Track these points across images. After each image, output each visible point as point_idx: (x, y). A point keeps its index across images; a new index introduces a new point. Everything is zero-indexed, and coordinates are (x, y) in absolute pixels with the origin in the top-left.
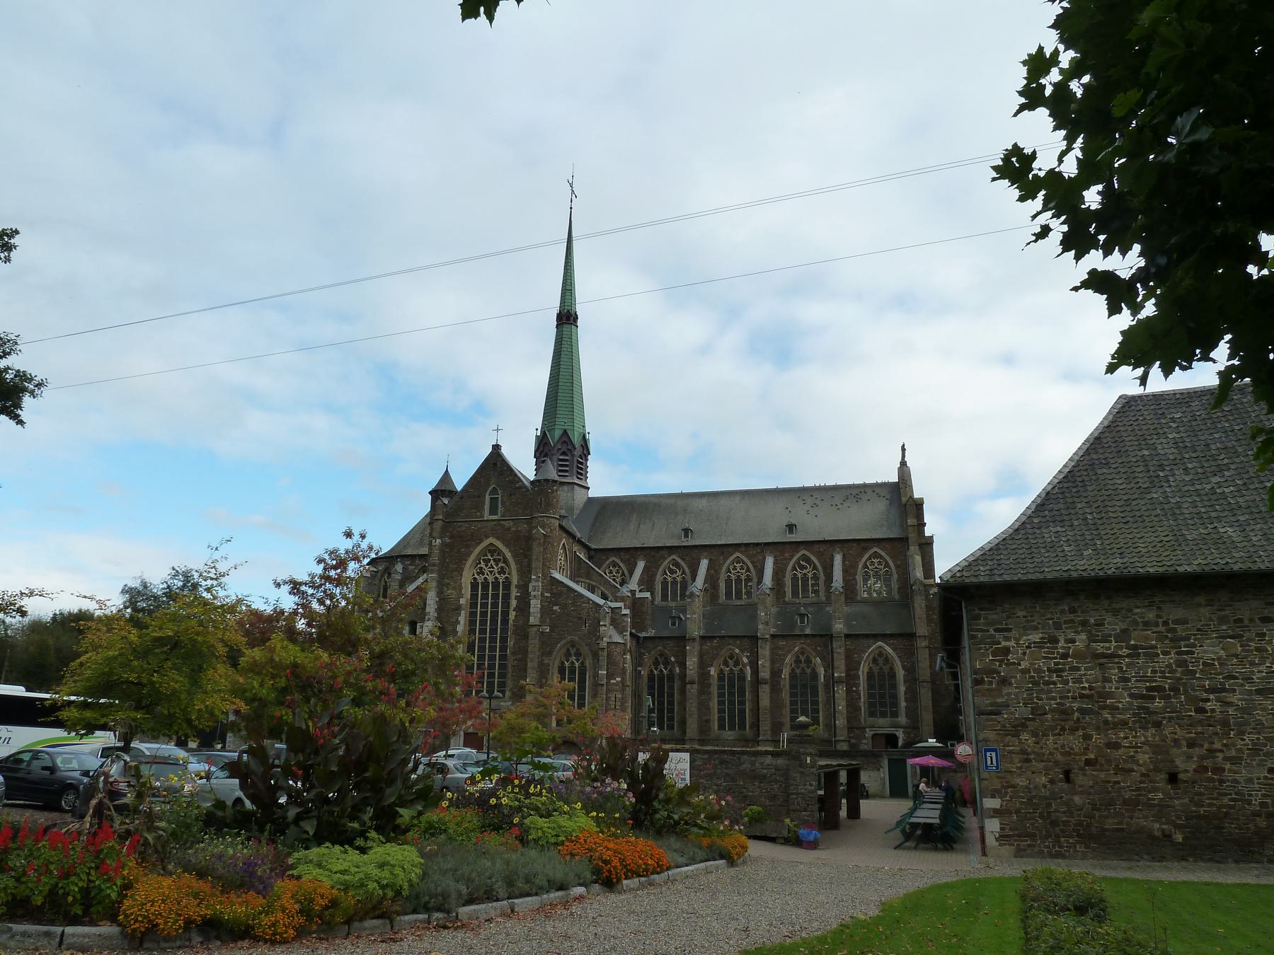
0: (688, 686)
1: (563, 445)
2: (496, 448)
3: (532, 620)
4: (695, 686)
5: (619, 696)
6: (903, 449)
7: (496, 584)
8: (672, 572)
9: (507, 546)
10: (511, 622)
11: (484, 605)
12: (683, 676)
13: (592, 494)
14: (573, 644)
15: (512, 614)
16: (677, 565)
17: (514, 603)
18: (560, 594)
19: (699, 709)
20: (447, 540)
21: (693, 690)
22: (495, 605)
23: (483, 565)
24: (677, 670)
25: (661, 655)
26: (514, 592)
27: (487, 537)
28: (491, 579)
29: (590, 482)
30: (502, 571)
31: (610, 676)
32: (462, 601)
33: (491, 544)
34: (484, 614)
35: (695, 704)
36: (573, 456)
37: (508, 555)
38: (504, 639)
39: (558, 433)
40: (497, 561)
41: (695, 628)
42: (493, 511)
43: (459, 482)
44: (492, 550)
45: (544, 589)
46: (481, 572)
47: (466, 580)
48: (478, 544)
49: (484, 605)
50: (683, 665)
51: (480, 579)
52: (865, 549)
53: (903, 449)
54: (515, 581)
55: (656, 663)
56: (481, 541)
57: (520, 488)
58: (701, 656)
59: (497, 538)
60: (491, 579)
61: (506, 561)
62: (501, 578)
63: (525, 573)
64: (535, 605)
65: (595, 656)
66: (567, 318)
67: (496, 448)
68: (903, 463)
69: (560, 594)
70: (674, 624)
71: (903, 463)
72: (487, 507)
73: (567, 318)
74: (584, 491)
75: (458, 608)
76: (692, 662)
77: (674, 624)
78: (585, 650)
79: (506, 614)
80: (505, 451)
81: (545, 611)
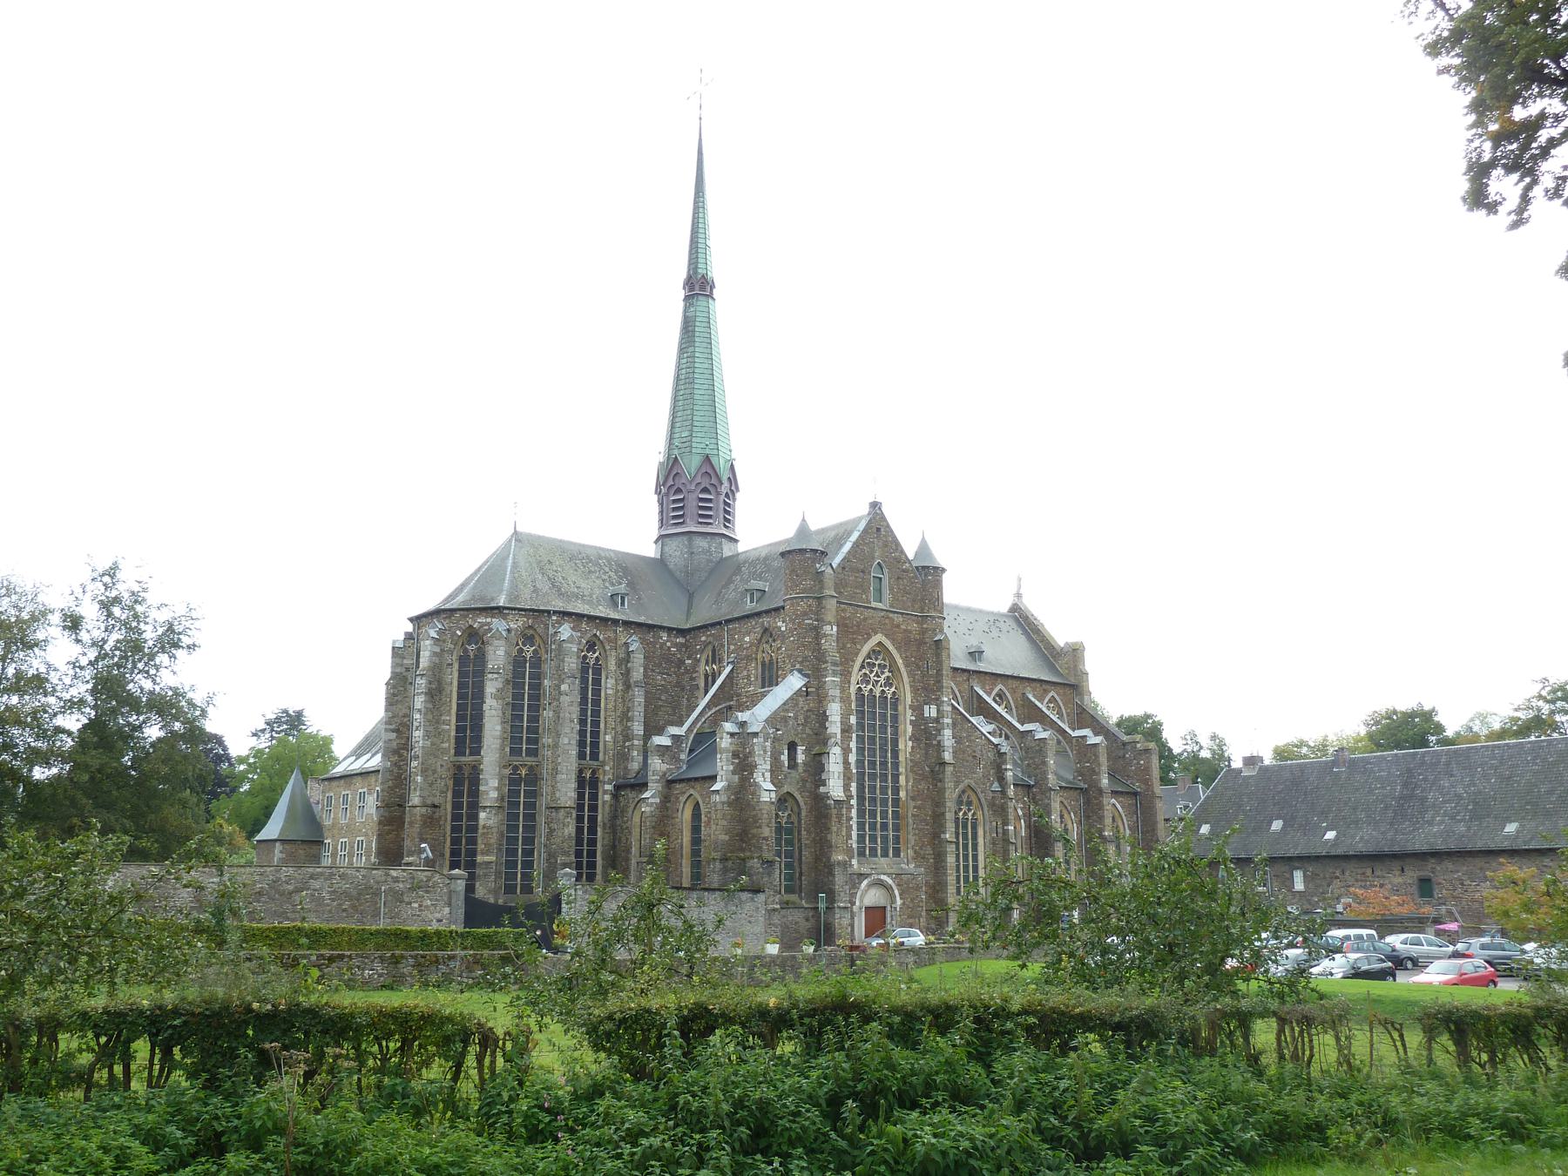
2: (875, 505)
30: (888, 683)
36: (718, 494)
37: (900, 662)
38: (896, 777)
39: (695, 462)
40: (882, 667)
51: (866, 689)
52: (1046, 692)
61: (893, 668)
62: (889, 692)
66: (698, 286)
67: (875, 505)
71: (1019, 595)
73: (698, 286)
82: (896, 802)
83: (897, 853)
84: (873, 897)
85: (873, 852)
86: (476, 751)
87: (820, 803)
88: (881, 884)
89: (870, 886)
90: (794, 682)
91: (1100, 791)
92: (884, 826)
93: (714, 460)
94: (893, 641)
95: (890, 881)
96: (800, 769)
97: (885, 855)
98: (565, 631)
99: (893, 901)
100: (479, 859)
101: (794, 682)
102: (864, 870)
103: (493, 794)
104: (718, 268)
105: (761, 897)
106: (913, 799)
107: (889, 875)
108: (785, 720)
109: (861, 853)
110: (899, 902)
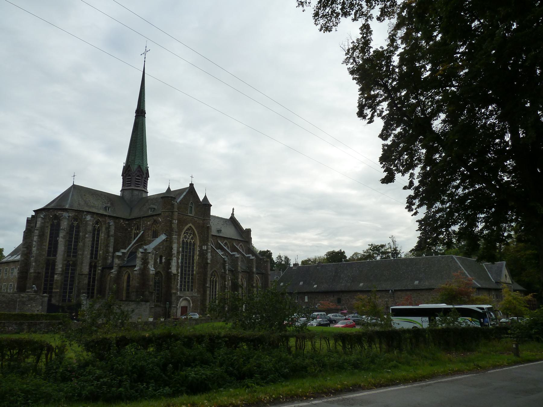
1: (135, 170)
2: (192, 185)
6: (233, 209)
7: (190, 243)
28: (189, 241)
30: (192, 239)
36: (142, 177)
37: (196, 232)
51: (185, 240)
52: (239, 243)
53: (233, 209)
60: (189, 241)
61: (194, 234)
66: (140, 113)
67: (192, 185)
68: (233, 214)
71: (233, 214)
73: (140, 113)
82: (193, 275)
83: (192, 290)
86: (55, 255)
87: (169, 276)
88: (186, 299)
89: (183, 300)
90: (163, 237)
91: (253, 273)
92: (188, 282)
93: (142, 167)
95: (189, 299)
96: (163, 264)
97: (188, 290)
98: (89, 218)
100: (54, 290)
101: (163, 237)
102: (181, 295)
103: (60, 270)
104: (147, 109)
105: (148, 304)
106: (198, 274)
108: (159, 248)
109: (181, 290)
110: (192, 305)
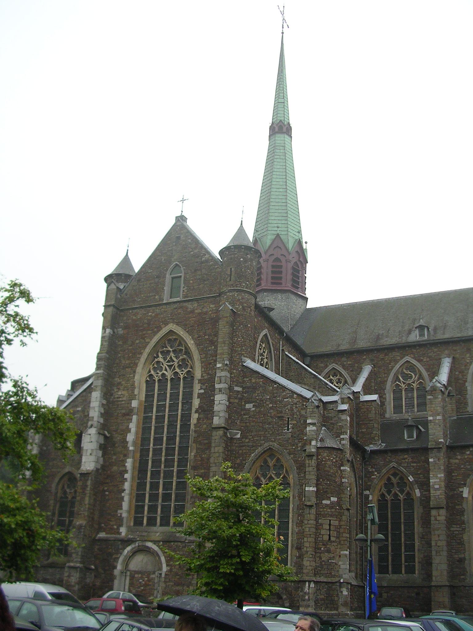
0: (434, 512)
2: (181, 220)
3: (216, 421)
4: (443, 512)
5: (335, 523)
7: (175, 380)
8: (407, 377)
9: (190, 332)
10: (192, 427)
11: (161, 408)
12: (426, 500)
13: (310, 305)
14: (270, 452)
15: (195, 417)
16: (412, 368)
17: (196, 402)
18: (254, 388)
19: (449, 544)
20: (120, 331)
21: (440, 517)
22: (173, 407)
23: (160, 359)
24: (417, 492)
25: (395, 475)
26: (197, 389)
27: (166, 324)
28: (169, 374)
29: (308, 294)
31: (320, 495)
32: (135, 404)
33: (171, 332)
34: (160, 419)
35: (443, 537)
37: (191, 343)
38: (184, 450)
41: (437, 434)
42: (173, 292)
43: (137, 265)
44: (171, 338)
45: (233, 381)
46: (158, 367)
47: (140, 377)
48: (155, 333)
49: (161, 408)
50: (425, 485)
54: (198, 374)
55: (389, 485)
56: (159, 329)
57: (207, 261)
58: (449, 473)
59: (177, 324)
60: (169, 374)
61: (188, 352)
63: (209, 366)
64: (220, 401)
65: (301, 467)
67: (181, 220)
69: (254, 388)
70: (411, 436)
72: (167, 289)
74: (301, 301)
75: (129, 413)
76: (437, 480)
77: (411, 436)
78: (288, 461)
79: (186, 417)
80: (193, 225)
81: (232, 409)
84: (139, 562)
85: (152, 522)
89: (134, 553)
94: (185, 327)
99: (160, 569)
107: (155, 542)
109: (138, 522)
110: (165, 568)
